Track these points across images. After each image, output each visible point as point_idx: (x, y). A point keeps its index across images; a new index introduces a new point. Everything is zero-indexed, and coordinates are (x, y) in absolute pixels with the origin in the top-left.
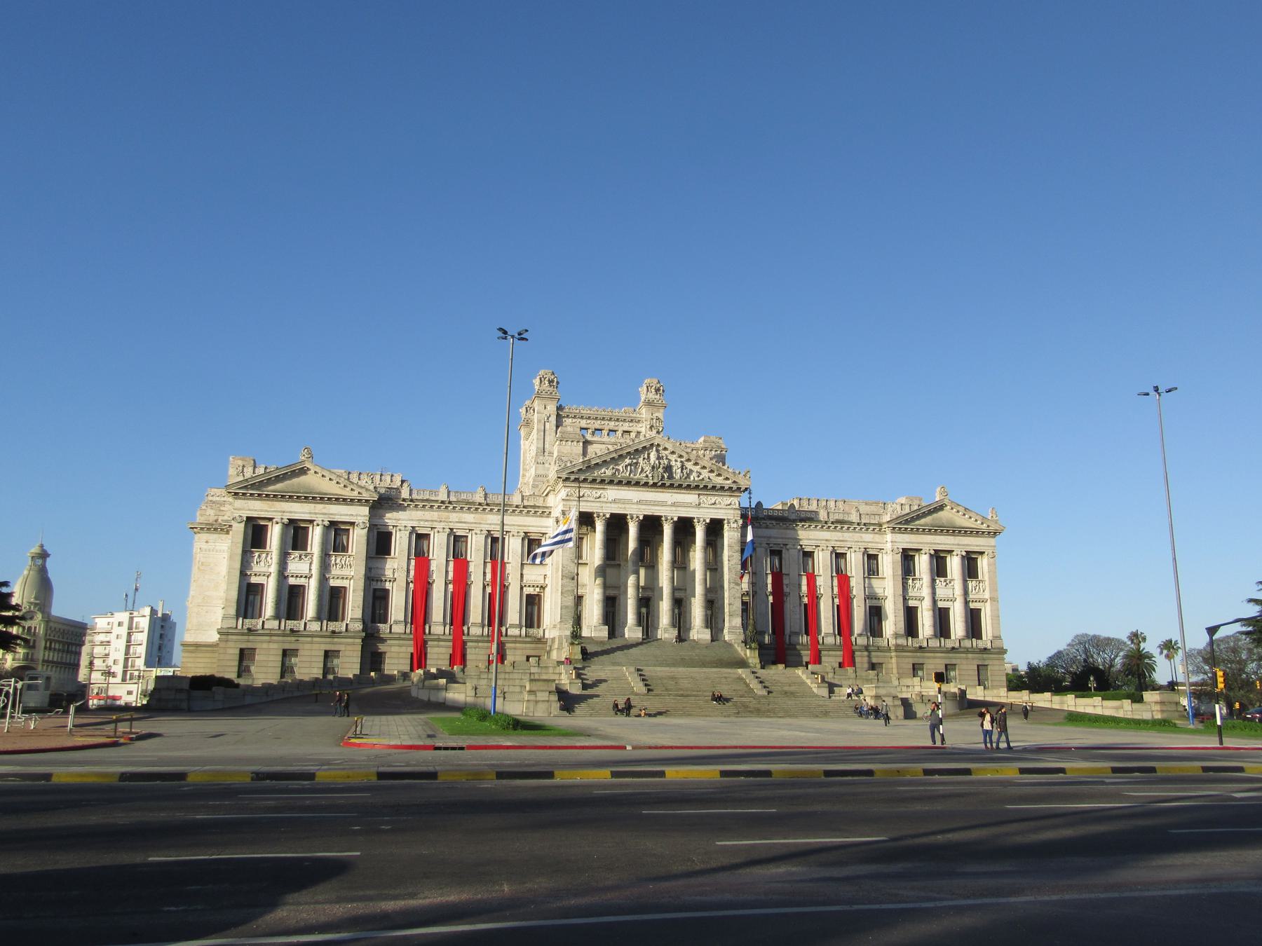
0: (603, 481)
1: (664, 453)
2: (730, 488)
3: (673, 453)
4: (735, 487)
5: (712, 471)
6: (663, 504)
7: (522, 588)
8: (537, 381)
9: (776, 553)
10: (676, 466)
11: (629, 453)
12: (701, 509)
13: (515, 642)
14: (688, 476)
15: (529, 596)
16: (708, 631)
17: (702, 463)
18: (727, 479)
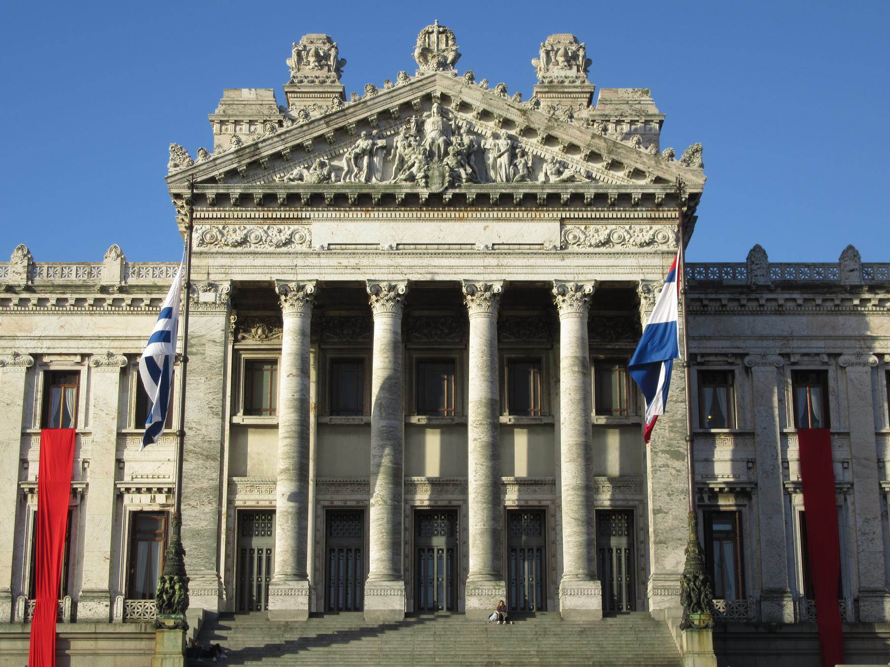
0: (292, 199)
1: (464, 118)
2: (648, 198)
3: (485, 115)
4: (659, 192)
5: (594, 156)
6: (464, 250)
7: (119, 497)
8: (291, 62)
9: (811, 378)
10: (495, 147)
11: (364, 123)
12: (570, 259)
13: (95, 636)
14: (531, 172)
15: (137, 516)
16: (595, 588)
17: (567, 135)
18: (637, 173)
